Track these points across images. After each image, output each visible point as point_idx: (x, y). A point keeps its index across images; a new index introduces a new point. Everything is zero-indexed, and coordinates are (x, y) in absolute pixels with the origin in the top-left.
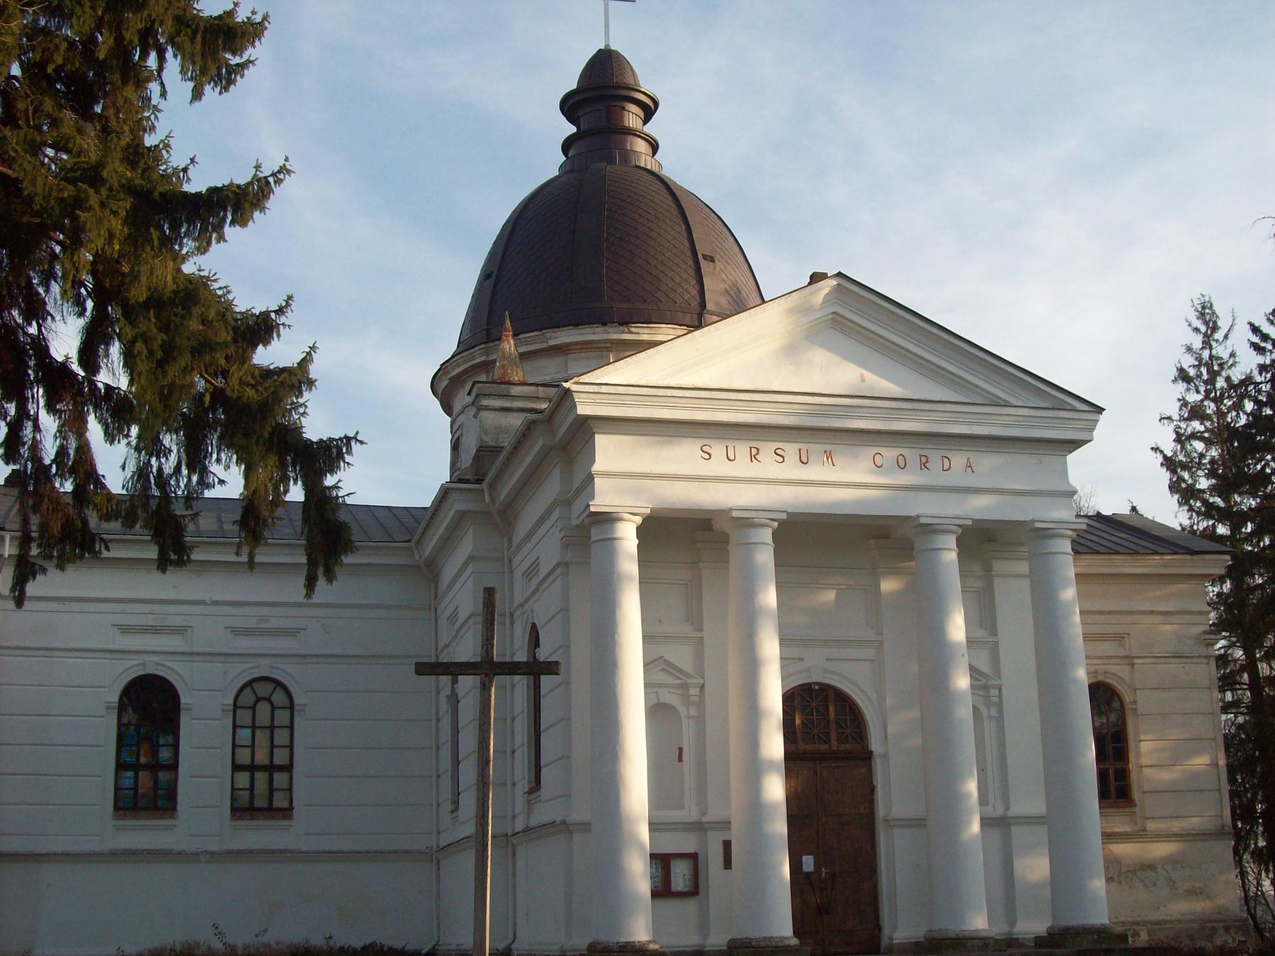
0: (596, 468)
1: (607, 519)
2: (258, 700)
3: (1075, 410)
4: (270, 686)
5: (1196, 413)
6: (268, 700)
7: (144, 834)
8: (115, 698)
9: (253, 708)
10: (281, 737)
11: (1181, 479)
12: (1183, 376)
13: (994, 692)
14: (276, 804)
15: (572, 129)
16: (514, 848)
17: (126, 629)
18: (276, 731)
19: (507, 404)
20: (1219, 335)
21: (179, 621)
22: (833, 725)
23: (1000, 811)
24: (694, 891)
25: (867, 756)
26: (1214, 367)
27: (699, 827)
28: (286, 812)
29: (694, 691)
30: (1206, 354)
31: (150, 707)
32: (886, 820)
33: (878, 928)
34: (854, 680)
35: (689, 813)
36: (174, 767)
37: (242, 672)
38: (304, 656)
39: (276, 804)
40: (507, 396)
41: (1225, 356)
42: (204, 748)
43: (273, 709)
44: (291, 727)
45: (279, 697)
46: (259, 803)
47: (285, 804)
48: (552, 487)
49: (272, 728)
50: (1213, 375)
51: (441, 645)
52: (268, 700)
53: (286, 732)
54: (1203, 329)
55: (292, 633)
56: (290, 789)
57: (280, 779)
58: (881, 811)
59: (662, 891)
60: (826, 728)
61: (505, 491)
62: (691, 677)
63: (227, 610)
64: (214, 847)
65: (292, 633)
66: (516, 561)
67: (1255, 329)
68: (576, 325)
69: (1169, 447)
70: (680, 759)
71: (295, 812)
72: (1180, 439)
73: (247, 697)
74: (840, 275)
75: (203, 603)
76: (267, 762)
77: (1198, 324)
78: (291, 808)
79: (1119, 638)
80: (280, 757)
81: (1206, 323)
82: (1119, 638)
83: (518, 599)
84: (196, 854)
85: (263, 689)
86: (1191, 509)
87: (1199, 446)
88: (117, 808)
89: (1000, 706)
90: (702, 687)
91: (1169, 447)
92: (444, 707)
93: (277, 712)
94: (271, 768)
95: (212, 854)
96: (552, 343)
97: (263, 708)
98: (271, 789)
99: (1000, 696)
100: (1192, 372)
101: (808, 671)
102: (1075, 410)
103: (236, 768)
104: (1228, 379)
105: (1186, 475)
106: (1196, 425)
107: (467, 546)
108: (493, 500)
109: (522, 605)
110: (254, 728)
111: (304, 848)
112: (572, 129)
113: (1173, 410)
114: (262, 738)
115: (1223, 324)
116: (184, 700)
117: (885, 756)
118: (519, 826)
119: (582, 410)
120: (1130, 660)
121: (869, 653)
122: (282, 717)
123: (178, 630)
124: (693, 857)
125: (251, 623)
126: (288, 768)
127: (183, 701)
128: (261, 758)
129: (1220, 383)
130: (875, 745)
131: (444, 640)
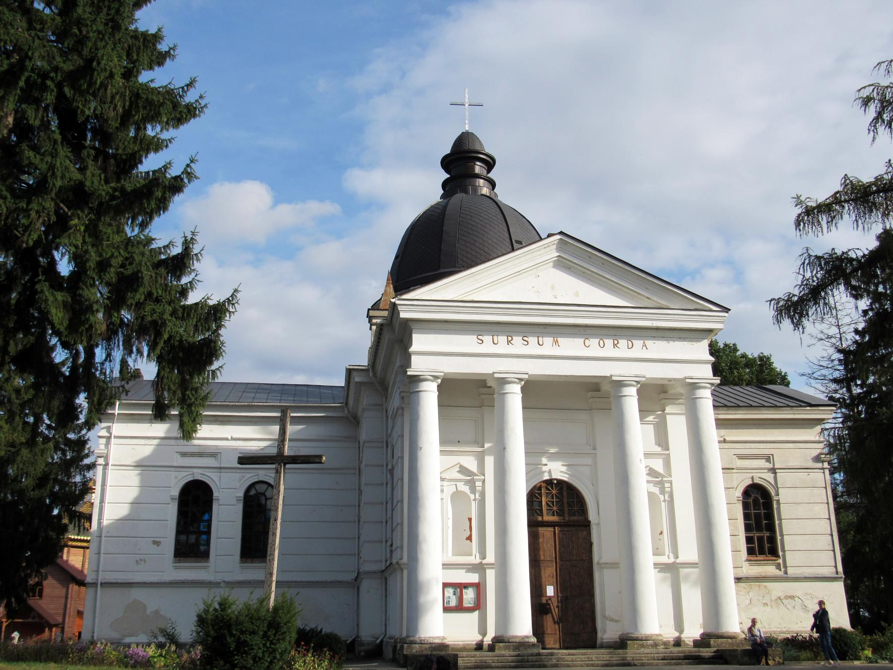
0: (412, 349)
1: (416, 380)
3: (711, 311)
4: (266, 486)
7: (190, 572)
8: (176, 492)
13: (667, 485)
16: (386, 579)
17: (184, 454)
22: (566, 505)
25: (587, 525)
27: (480, 568)
31: (195, 500)
32: (598, 563)
33: (594, 630)
35: (475, 559)
36: (208, 533)
42: (226, 521)
58: (596, 558)
62: (476, 475)
64: (229, 578)
74: (561, 233)
75: (227, 439)
79: (768, 459)
82: (768, 459)
99: (671, 487)
102: (711, 311)
116: (215, 494)
117: (598, 524)
119: (403, 315)
120: (773, 471)
121: (588, 461)
127: (215, 495)
130: (592, 516)
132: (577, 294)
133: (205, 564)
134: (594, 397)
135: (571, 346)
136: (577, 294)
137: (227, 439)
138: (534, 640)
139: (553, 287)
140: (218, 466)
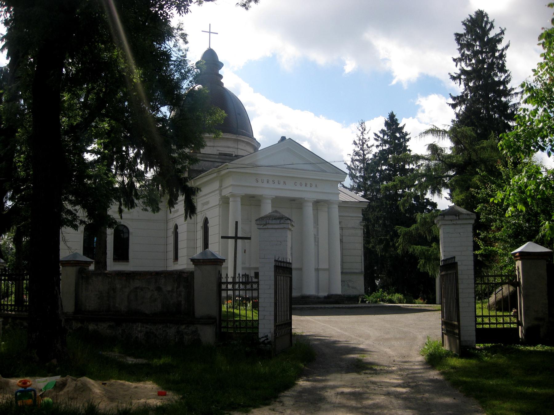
3: (341, 174)
5: (357, 154)
11: (352, 172)
12: (355, 143)
20: (366, 132)
26: (363, 142)
27: (250, 269)
30: (361, 137)
35: (247, 265)
41: (367, 138)
48: (216, 185)
50: (363, 143)
54: (361, 130)
67: (376, 135)
69: (349, 163)
70: (245, 252)
72: (353, 161)
77: (360, 128)
86: (354, 182)
87: (357, 163)
89: (318, 242)
91: (349, 163)
100: (357, 142)
102: (341, 174)
104: (367, 145)
105: (353, 172)
106: (357, 158)
113: (352, 153)
115: (367, 129)
129: (365, 146)
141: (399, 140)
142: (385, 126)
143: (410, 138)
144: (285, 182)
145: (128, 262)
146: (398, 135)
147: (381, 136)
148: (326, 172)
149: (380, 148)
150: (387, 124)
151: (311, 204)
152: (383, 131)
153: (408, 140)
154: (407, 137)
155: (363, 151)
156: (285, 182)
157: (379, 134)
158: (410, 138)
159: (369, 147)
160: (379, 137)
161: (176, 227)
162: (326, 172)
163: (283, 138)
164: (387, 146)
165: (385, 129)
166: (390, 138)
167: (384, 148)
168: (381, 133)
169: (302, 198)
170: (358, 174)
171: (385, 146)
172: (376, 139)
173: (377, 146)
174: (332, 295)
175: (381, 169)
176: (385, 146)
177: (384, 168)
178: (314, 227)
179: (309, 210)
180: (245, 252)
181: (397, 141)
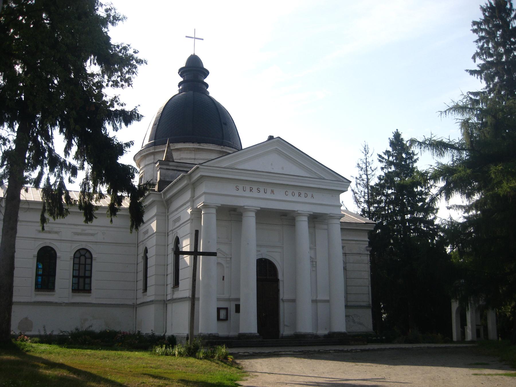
2: (81, 255)
3: (343, 181)
4: (85, 251)
6: (84, 255)
8: (36, 253)
9: (80, 258)
10: (88, 267)
14: (86, 288)
15: (182, 79)
16: (166, 304)
18: (87, 266)
19: (168, 167)
20: (369, 155)
21: (56, 230)
23: (314, 298)
24: (226, 319)
25: (277, 281)
27: (229, 300)
28: (89, 291)
29: (228, 259)
31: (47, 257)
32: (282, 300)
33: (278, 331)
34: (276, 258)
35: (226, 296)
37: (76, 247)
38: (96, 242)
39: (86, 288)
40: (168, 165)
43: (86, 258)
44: (91, 264)
45: (87, 255)
46: (81, 287)
47: (89, 288)
48: (188, 195)
49: (85, 264)
51: (140, 240)
52: (84, 255)
53: (90, 266)
54: (365, 152)
55: (92, 235)
56: (90, 284)
57: (87, 280)
58: (281, 297)
59: (219, 319)
60: (267, 272)
61: (168, 196)
63: (73, 227)
64: (66, 301)
65: (92, 235)
66: (170, 217)
68: (184, 142)
70: (223, 279)
71: (92, 291)
73: (78, 255)
75: (65, 224)
76: (83, 275)
78: (91, 290)
80: (88, 274)
81: (365, 150)
83: (170, 229)
84: (61, 303)
85: (83, 252)
88: (36, 288)
89: (316, 267)
90: (231, 258)
92: (141, 260)
93: (87, 260)
94: (85, 277)
95: (67, 303)
96: (176, 147)
97: (83, 258)
98: (85, 284)
99: (316, 264)
101: (262, 254)
102: (343, 181)
103: (74, 277)
107: (154, 211)
108: (164, 197)
109: (172, 230)
110: (79, 264)
111: (94, 302)
112: (182, 79)
114: (82, 267)
115: (370, 153)
116: (58, 254)
117: (283, 281)
118: (169, 297)
122: (88, 261)
123: (56, 233)
124: (226, 309)
125: (79, 231)
126: (90, 277)
128: (82, 274)
129: (369, 169)
130: (280, 277)
131: (141, 238)
132: (283, 168)
133: (53, 293)
134: (288, 218)
135: (279, 194)
136: (283, 168)
137: (65, 224)
138: (258, 334)
139: (272, 164)
140: (60, 239)
141: (406, 162)
142: (390, 146)
143: (417, 159)
144: (272, 192)
145: (90, 293)
146: (404, 156)
147: (386, 157)
148: (324, 179)
149: (386, 171)
150: (392, 144)
151: (306, 219)
152: (387, 153)
153: (415, 161)
154: (415, 157)
155: (367, 175)
156: (272, 192)
157: (383, 156)
158: (417, 159)
159: (373, 171)
160: (383, 158)
161: (146, 251)
162: (324, 179)
163: (271, 138)
164: (393, 168)
165: (390, 149)
166: (396, 159)
167: (390, 170)
168: (385, 154)
169: (294, 211)
170: (362, 200)
171: (391, 168)
172: (380, 161)
173: (382, 169)
174: (334, 333)
175: (387, 193)
176: (391, 168)
177: (390, 191)
178: (310, 248)
179: (303, 225)
180: (223, 279)
181: (403, 163)
